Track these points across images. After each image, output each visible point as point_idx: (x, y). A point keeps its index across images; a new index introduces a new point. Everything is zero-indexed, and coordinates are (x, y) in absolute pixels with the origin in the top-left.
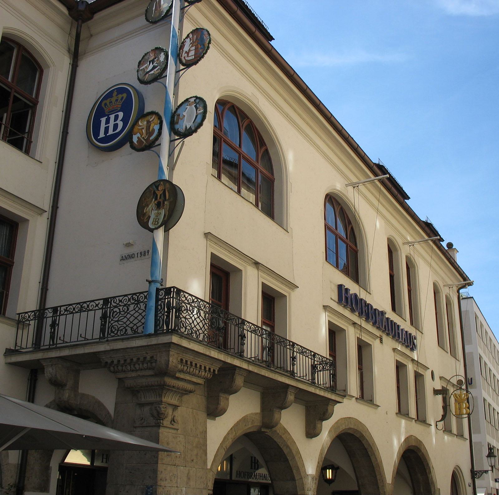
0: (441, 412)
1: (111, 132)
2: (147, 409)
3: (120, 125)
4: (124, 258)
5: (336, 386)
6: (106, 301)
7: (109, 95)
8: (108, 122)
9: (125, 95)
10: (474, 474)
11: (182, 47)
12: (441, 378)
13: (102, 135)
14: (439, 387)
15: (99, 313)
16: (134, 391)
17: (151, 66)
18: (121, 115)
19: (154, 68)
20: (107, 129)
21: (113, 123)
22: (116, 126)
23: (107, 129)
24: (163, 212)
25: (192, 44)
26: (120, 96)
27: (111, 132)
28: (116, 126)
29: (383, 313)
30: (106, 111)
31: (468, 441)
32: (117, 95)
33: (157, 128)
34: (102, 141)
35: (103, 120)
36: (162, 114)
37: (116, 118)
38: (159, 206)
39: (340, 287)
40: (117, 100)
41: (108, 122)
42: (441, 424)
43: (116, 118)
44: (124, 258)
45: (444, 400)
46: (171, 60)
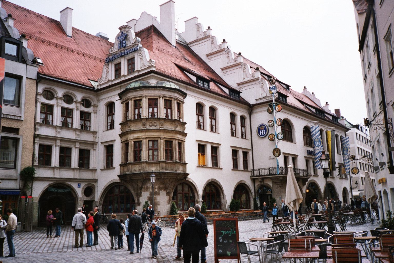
1: (263, 134)
2: (278, 186)
4: (269, 159)
5: (308, 175)
6: (269, 168)
7: (261, 126)
8: (261, 132)
10: (351, 189)
11: (277, 121)
13: (261, 134)
15: (268, 170)
16: (275, 183)
17: (271, 124)
18: (264, 131)
19: (271, 124)
20: (262, 133)
21: (262, 132)
22: (264, 133)
23: (262, 133)
24: (278, 154)
25: (279, 121)
27: (263, 134)
28: (264, 133)
31: (349, 180)
33: (274, 137)
35: (260, 131)
36: (275, 134)
37: (263, 131)
38: (277, 153)
39: (308, 150)
41: (261, 132)
43: (263, 131)
44: (269, 159)
46: (275, 124)
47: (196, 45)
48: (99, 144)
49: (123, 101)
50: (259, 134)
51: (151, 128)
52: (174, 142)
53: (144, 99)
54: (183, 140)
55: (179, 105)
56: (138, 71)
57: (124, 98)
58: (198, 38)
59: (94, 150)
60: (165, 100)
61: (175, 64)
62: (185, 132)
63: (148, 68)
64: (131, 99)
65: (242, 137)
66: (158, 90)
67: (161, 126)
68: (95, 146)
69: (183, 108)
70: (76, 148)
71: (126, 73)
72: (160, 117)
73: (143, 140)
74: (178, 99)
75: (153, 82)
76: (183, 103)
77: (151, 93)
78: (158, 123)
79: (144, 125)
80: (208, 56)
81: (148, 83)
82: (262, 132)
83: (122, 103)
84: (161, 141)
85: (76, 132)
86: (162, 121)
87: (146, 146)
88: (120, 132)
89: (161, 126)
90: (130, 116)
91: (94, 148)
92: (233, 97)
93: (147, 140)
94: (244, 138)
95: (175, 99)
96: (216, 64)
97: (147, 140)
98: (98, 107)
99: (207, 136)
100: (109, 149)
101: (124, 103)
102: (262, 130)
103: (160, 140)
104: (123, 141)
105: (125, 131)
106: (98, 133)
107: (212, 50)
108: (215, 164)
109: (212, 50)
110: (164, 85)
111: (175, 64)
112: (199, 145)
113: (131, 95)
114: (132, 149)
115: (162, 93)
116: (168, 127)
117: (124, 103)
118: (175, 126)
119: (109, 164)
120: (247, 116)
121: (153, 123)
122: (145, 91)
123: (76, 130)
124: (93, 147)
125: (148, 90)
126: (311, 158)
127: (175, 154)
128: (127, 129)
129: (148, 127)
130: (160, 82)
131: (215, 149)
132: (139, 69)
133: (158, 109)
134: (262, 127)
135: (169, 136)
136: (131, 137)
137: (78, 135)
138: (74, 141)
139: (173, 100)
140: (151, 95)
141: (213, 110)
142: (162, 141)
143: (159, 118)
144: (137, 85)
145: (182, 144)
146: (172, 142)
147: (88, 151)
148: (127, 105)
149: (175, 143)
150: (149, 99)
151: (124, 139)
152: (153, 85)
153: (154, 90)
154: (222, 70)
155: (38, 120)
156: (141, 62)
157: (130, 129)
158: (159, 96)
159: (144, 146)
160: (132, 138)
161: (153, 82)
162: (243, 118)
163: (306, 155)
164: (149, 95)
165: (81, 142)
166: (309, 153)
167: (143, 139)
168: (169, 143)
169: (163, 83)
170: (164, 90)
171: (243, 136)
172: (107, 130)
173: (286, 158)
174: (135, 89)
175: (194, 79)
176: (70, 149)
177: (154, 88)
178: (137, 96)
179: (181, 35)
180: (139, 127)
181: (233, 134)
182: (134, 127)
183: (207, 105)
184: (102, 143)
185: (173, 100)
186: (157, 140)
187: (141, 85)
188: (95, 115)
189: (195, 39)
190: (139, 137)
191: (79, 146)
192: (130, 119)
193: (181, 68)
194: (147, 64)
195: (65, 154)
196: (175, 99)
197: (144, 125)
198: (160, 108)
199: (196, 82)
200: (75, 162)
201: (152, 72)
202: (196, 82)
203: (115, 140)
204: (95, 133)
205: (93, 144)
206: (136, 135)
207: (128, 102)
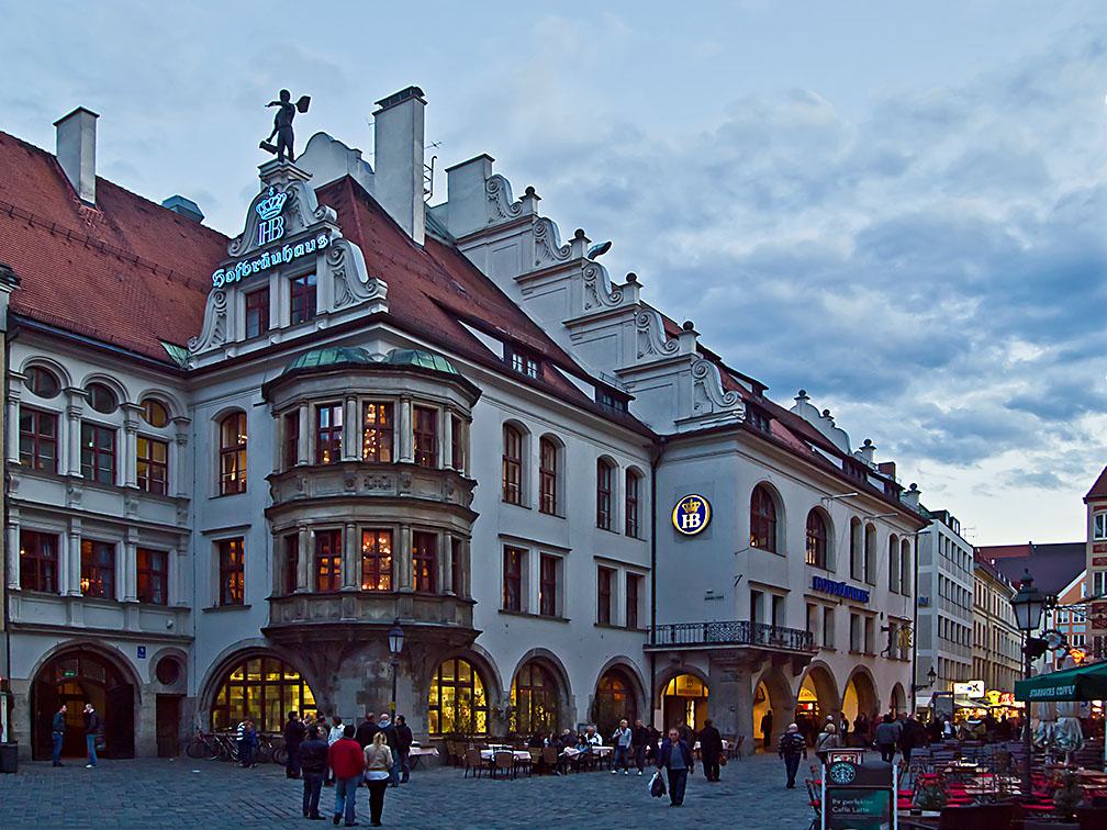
0: (887, 645)
1: (691, 525)
3: (698, 523)
7: (687, 501)
8: (688, 518)
12: (890, 617)
13: (685, 526)
14: (887, 626)
18: (698, 516)
20: (688, 524)
22: (695, 523)
23: (688, 524)
26: (695, 503)
28: (695, 523)
29: (843, 584)
31: (912, 663)
34: (685, 529)
35: (685, 517)
37: (694, 517)
39: (815, 578)
41: (688, 518)
42: (886, 654)
43: (694, 517)
45: (890, 635)
47: (485, 247)
48: (197, 534)
49: (277, 408)
50: (681, 523)
51: (372, 493)
52: (440, 537)
53: (352, 403)
54: (466, 532)
55: (455, 422)
56: (329, 316)
57: (283, 399)
58: (491, 225)
59: (179, 551)
60: (416, 407)
61: (430, 298)
62: (473, 508)
63: (364, 306)
64: (306, 402)
65: (628, 533)
66: (393, 376)
67: (402, 489)
68: (183, 541)
69: (467, 435)
70: (127, 544)
71: (286, 323)
72: (402, 461)
73: (346, 528)
74: (458, 407)
75: (380, 352)
76: (470, 420)
77: (372, 384)
78: (394, 478)
79: (350, 483)
80: (521, 281)
81: (364, 352)
82: (691, 520)
83: (275, 414)
84: (401, 533)
85: (126, 497)
86: (406, 473)
87: (356, 544)
88: (271, 503)
89: (402, 489)
90: (305, 455)
91: (182, 548)
92: (607, 409)
93: (360, 528)
94: (631, 536)
95: (446, 407)
96: (547, 311)
97: (360, 528)
98: (191, 425)
99: (530, 525)
100: (229, 552)
101: (282, 415)
103: (401, 529)
104: (277, 528)
105: (284, 500)
106: (191, 502)
107: (538, 263)
108: (550, 610)
109: (538, 263)
110: (414, 362)
111: (430, 298)
112: (507, 549)
113: (304, 389)
114: (311, 555)
115: (408, 387)
116: (426, 490)
117: (282, 415)
118: (444, 489)
119: (231, 598)
120: (645, 468)
121: (378, 478)
122: (353, 378)
123: (126, 490)
124: (178, 545)
125: (365, 375)
126: (822, 600)
127: (444, 571)
128: (290, 494)
129: (362, 490)
130: (401, 351)
131: (551, 563)
132: (332, 310)
133: (395, 435)
135: (426, 517)
136: (309, 516)
137: (134, 507)
138: (121, 525)
139: (440, 410)
140: (374, 391)
141: (550, 444)
142: (405, 531)
143: (398, 463)
144: (327, 358)
145: (463, 544)
146: (436, 535)
147: (164, 556)
148: (293, 420)
149: (444, 541)
150: (366, 404)
151: (282, 522)
152: (380, 360)
153: (384, 376)
154: (569, 328)
155: (15, 457)
156: (338, 287)
157: (303, 492)
158: (400, 395)
159: (350, 546)
160: (310, 521)
161: (381, 351)
162: (632, 475)
163: (810, 592)
164: (368, 391)
165: (145, 528)
166: (818, 584)
167: (346, 524)
168: (424, 540)
169: (410, 356)
170: (414, 377)
171: (632, 530)
172: (222, 495)
173: (755, 596)
174: (322, 371)
175: (497, 348)
176: (111, 548)
177: (384, 369)
178: (327, 393)
179: (436, 213)
180: (336, 488)
181: (604, 521)
182: (313, 489)
183: (536, 431)
184: (205, 533)
185: (440, 410)
186: (391, 531)
187: (342, 359)
188: (182, 448)
189: (481, 224)
190: (332, 520)
191: (137, 541)
192: (304, 463)
193: (452, 314)
194: (362, 295)
195: (98, 561)
196: (446, 407)
197: (350, 483)
198: (403, 433)
199: (501, 356)
200: (127, 587)
201: (379, 318)
202: (501, 356)
203: (249, 526)
204: (181, 502)
205: (178, 535)
206: (323, 514)
207: (297, 413)
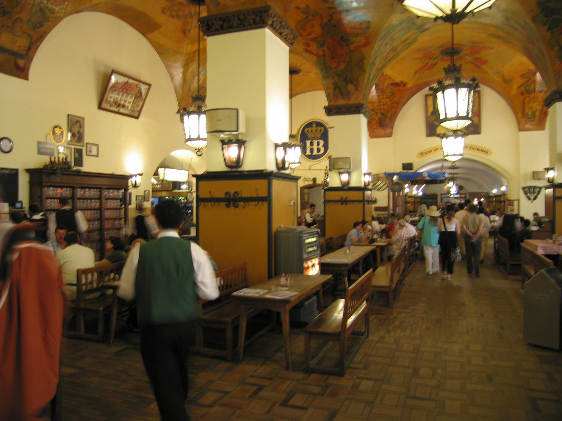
1: (315, 152)
7: (310, 125)
8: (312, 144)
9: (323, 129)
13: (308, 153)
18: (322, 142)
20: (312, 150)
22: (319, 150)
23: (312, 150)
26: (319, 129)
27: (315, 152)
28: (319, 150)
30: (310, 136)
32: (316, 127)
35: (308, 143)
37: (318, 144)
40: (317, 131)
41: (312, 144)
43: (318, 144)
82: (315, 147)
102: (316, 138)
134: (314, 129)
